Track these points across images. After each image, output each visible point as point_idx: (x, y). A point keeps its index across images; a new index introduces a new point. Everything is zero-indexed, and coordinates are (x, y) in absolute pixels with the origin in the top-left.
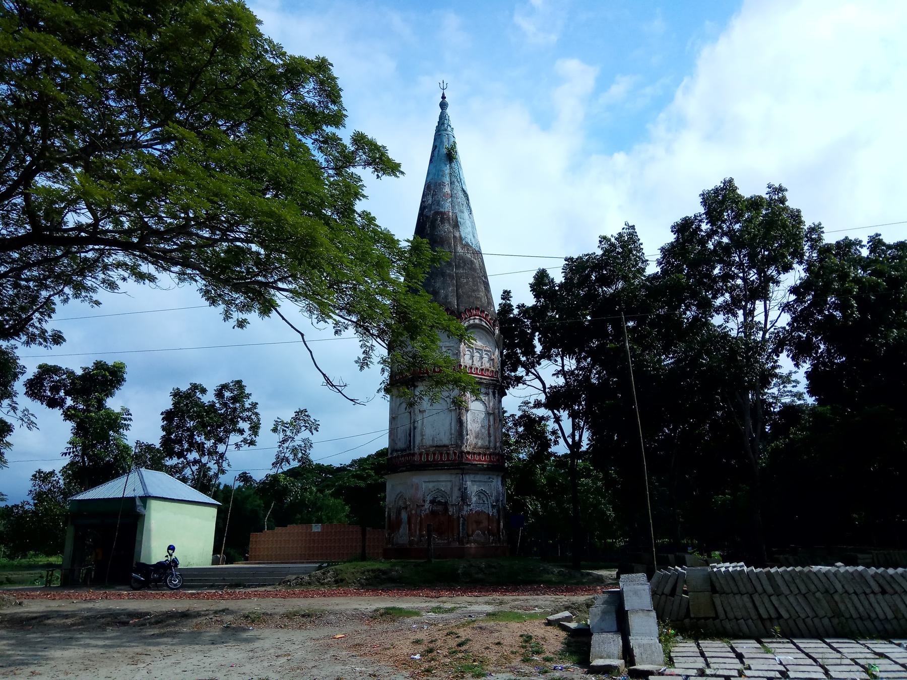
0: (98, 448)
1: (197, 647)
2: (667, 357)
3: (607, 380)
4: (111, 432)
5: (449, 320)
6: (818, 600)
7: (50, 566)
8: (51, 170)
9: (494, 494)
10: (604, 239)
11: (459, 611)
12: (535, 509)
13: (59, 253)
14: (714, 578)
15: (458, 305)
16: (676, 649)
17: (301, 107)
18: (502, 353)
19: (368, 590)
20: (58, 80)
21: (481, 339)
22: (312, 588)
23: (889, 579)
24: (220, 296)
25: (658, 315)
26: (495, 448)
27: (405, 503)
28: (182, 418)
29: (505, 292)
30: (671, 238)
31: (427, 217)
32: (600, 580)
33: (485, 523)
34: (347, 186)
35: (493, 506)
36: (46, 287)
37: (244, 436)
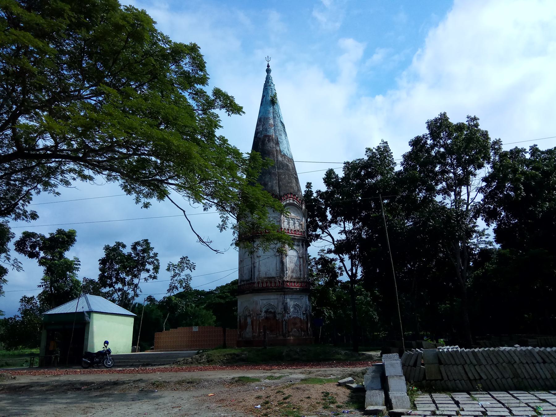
0: (60, 282)
1: (124, 403)
2: (408, 221)
3: (372, 236)
4: (68, 273)
5: (274, 201)
6: (504, 368)
7: (32, 355)
8: (29, 114)
9: (304, 306)
10: (369, 150)
11: (284, 378)
12: (330, 316)
13: (34, 164)
14: (440, 356)
16: (418, 399)
17: (182, 73)
18: (307, 220)
19: (227, 366)
20: (32, 59)
21: (294, 212)
22: (193, 365)
23: (547, 354)
24: (133, 188)
25: (402, 196)
26: (304, 278)
27: (249, 313)
28: (111, 263)
29: (308, 183)
30: (409, 149)
31: (260, 138)
32: (370, 358)
33: (299, 325)
34: (211, 121)
35: (304, 314)
36: (27, 185)
37: (150, 273)
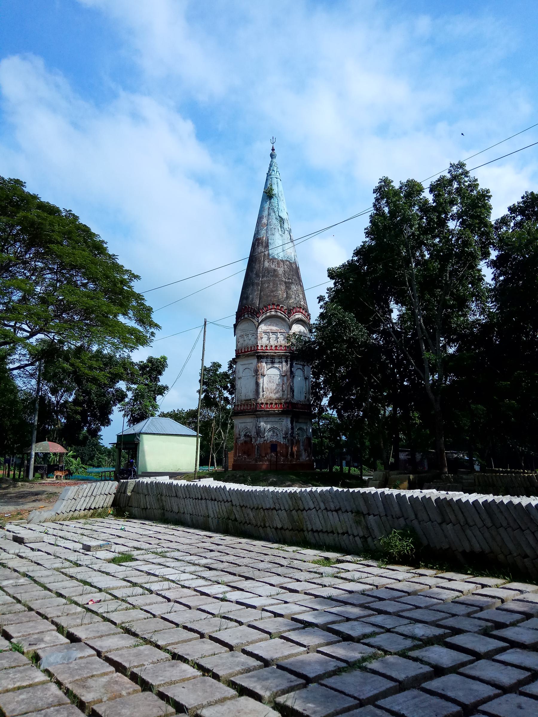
9: (284, 429)
15: (259, 304)
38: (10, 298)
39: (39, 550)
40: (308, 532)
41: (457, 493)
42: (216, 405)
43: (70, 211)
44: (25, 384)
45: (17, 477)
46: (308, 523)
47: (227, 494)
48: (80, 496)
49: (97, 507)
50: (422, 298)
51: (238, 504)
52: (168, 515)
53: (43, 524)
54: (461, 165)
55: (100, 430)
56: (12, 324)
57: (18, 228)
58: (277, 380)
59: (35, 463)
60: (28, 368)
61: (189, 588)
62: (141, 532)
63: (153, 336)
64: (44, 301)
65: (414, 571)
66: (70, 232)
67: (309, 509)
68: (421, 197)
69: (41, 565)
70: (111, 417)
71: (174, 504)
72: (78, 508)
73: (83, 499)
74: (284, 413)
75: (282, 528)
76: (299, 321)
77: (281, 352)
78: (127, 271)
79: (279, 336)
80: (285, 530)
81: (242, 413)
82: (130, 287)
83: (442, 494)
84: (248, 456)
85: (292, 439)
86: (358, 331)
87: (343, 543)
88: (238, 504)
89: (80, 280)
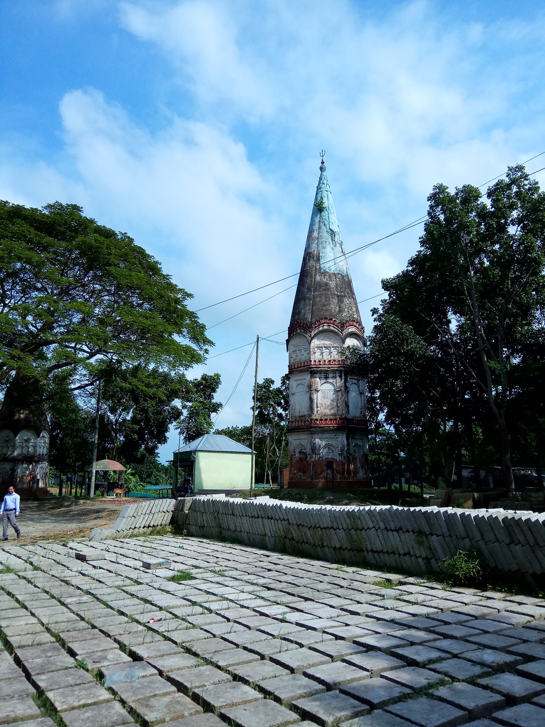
38: (71, 321)
39: (100, 568)
40: (368, 552)
41: (526, 512)
42: (270, 421)
43: (126, 233)
44: (86, 403)
45: (79, 495)
46: (368, 543)
47: (284, 512)
48: (139, 514)
49: (156, 525)
50: (482, 307)
51: (295, 523)
52: (226, 533)
53: (104, 542)
54: (520, 168)
55: (156, 447)
56: (73, 345)
57: (77, 252)
58: (331, 395)
59: (95, 481)
60: (88, 388)
61: (248, 608)
62: (199, 550)
63: (207, 353)
64: (102, 322)
65: (481, 594)
66: (126, 255)
67: (369, 528)
68: (479, 202)
69: (103, 583)
70: (167, 434)
71: (230, 522)
72: (138, 526)
73: (142, 516)
74: (339, 429)
75: (340, 548)
76: (352, 335)
77: (335, 367)
78: (180, 290)
79: (332, 350)
80: (344, 550)
81: (296, 429)
82: (184, 306)
83: (510, 514)
84: (304, 473)
85: (348, 456)
86: (416, 344)
87: (404, 565)
88: (295, 523)
89: (135, 300)
